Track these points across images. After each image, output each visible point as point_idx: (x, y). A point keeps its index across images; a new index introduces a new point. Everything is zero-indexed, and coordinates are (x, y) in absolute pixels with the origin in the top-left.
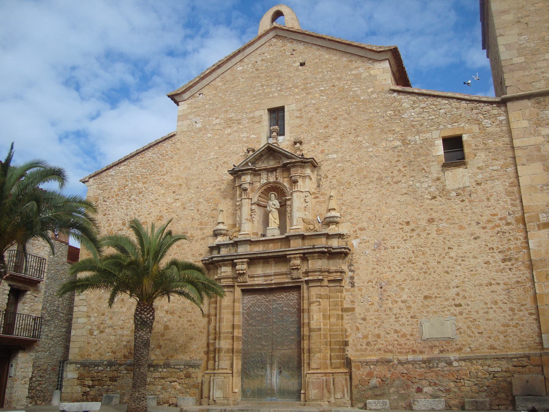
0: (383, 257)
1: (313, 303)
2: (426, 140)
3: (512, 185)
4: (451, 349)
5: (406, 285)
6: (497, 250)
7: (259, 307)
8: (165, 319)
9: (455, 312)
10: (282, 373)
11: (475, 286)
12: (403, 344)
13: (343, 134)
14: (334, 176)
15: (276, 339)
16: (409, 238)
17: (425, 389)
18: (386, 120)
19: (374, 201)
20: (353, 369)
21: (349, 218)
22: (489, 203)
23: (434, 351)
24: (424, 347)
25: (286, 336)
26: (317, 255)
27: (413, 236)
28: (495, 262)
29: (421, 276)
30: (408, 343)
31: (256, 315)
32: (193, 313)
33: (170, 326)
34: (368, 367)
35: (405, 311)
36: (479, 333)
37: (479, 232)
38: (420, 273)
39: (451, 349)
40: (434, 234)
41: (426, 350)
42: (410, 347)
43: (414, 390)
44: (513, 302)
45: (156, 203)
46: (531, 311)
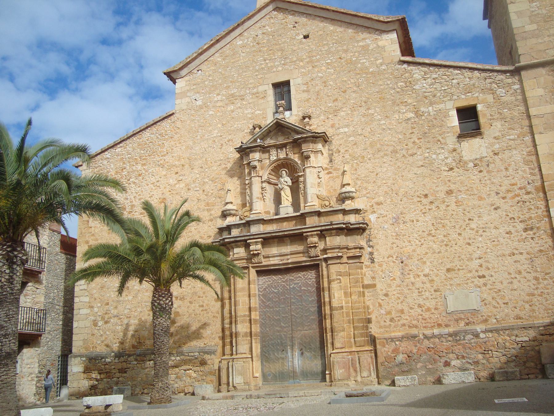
0: (402, 231)
1: (334, 280)
2: (439, 111)
3: (529, 154)
4: (477, 321)
5: (428, 259)
6: (518, 219)
7: (275, 288)
10: (304, 354)
11: (498, 256)
13: (353, 107)
14: (346, 151)
15: (296, 320)
16: (428, 211)
17: (453, 363)
18: (398, 92)
19: (390, 174)
20: (378, 347)
21: (365, 193)
22: (508, 173)
23: (460, 323)
24: (449, 320)
26: (335, 231)
27: (432, 209)
28: (517, 231)
29: (442, 248)
30: (433, 317)
31: (272, 297)
32: (204, 298)
33: (181, 313)
34: (393, 343)
35: (428, 285)
36: (504, 304)
37: (499, 202)
38: (441, 246)
40: (453, 206)
41: (451, 323)
42: (435, 321)
43: (441, 364)
44: (537, 271)
45: (158, 185)
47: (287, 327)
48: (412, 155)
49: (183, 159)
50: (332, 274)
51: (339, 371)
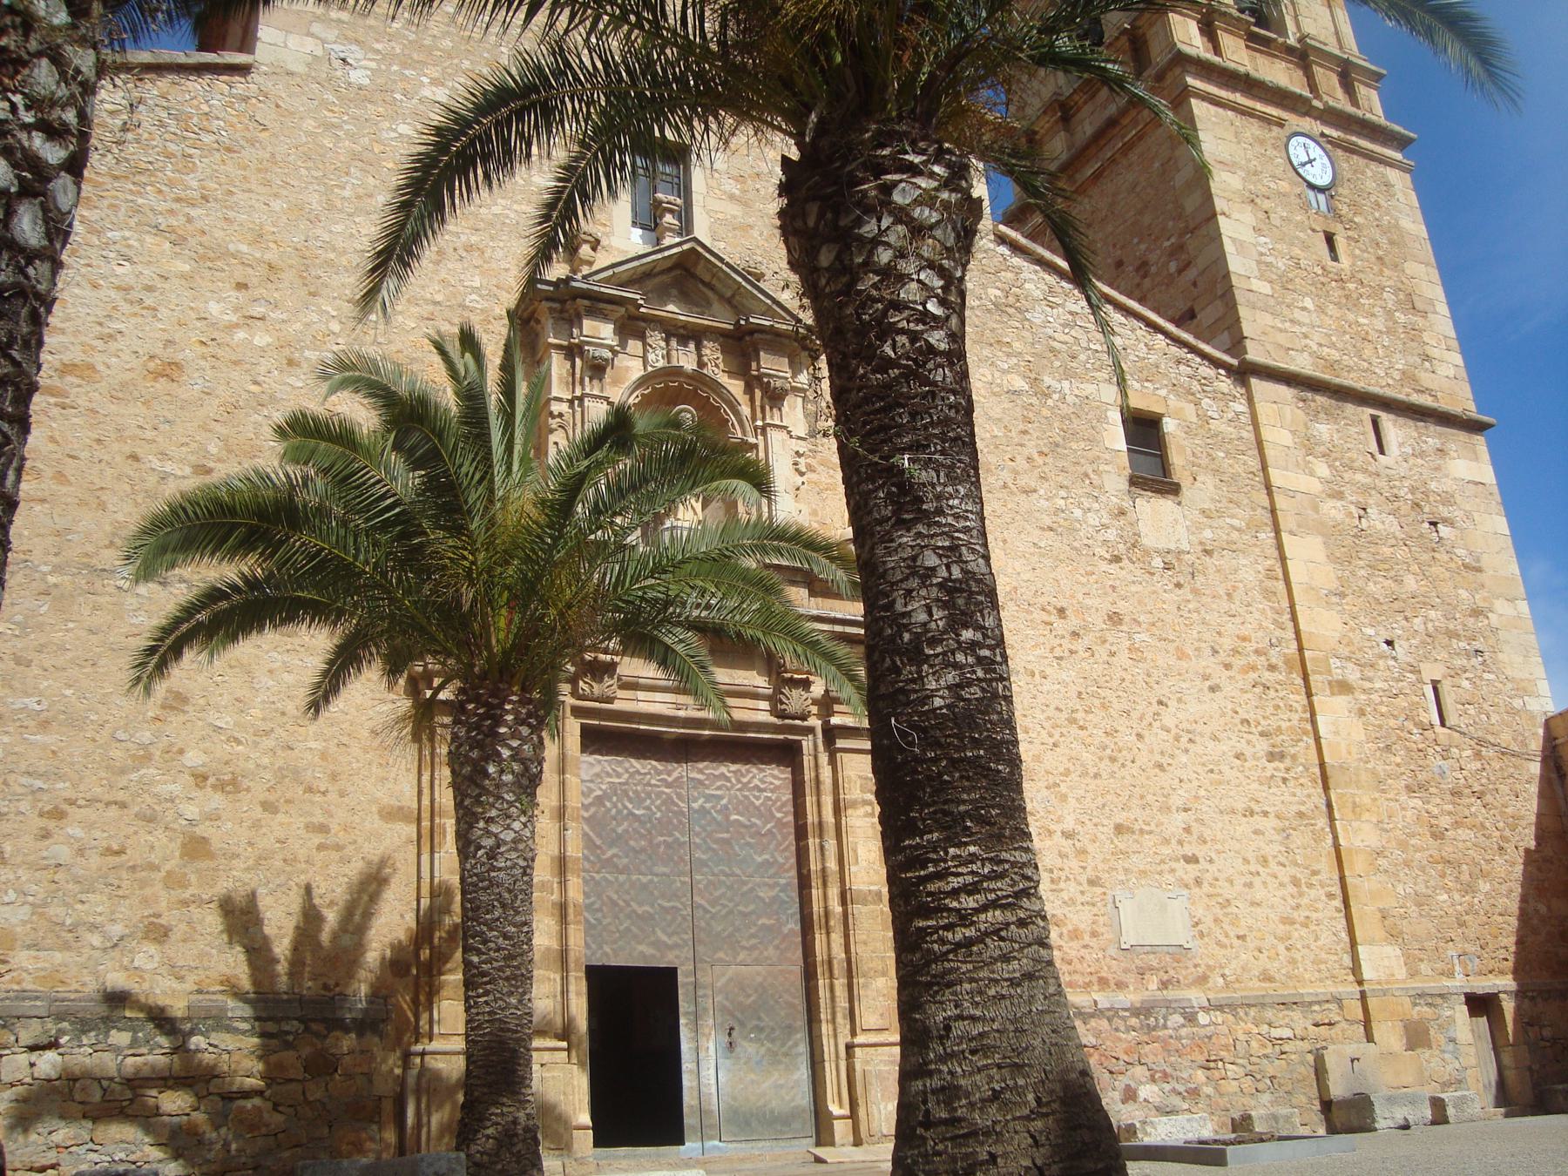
1: (854, 804)
5: (1071, 788)
7: (639, 801)
8: (191, 811)
9: (1185, 877)
10: (738, 1049)
12: (1075, 960)
15: (708, 924)
16: (1067, 654)
17: (1147, 1091)
24: (1126, 971)
25: (745, 915)
27: (1076, 652)
29: (1101, 766)
30: (1087, 957)
31: (626, 831)
32: (333, 796)
33: (216, 844)
35: (1074, 863)
37: (1220, 676)
38: (1101, 759)
39: (1185, 978)
40: (1123, 658)
41: (1131, 979)
44: (1296, 864)
45: (149, 302)
46: (1330, 889)
47: (676, 946)
48: (1026, 492)
49: (272, 245)
50: (849, 782)
51: (885, 1108)
